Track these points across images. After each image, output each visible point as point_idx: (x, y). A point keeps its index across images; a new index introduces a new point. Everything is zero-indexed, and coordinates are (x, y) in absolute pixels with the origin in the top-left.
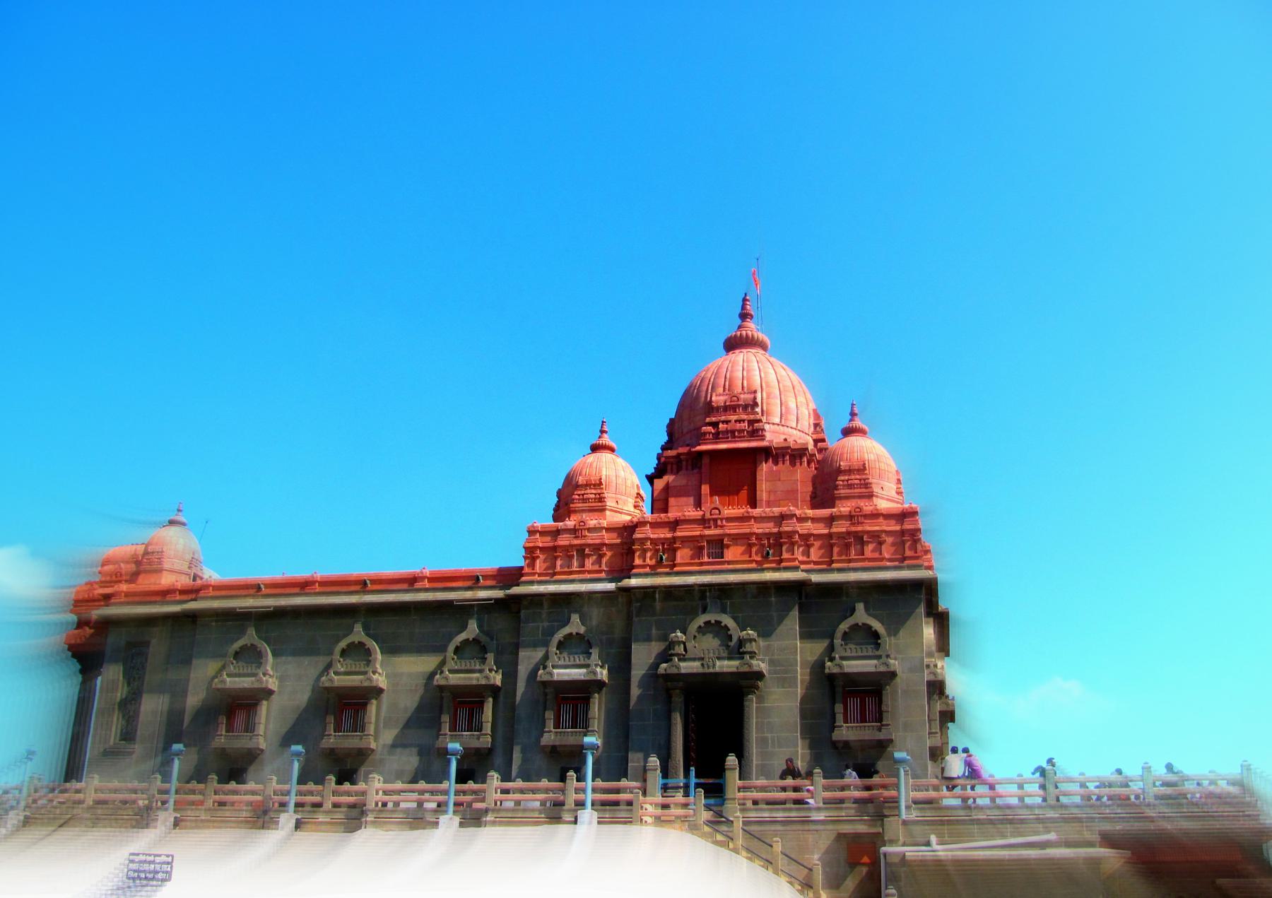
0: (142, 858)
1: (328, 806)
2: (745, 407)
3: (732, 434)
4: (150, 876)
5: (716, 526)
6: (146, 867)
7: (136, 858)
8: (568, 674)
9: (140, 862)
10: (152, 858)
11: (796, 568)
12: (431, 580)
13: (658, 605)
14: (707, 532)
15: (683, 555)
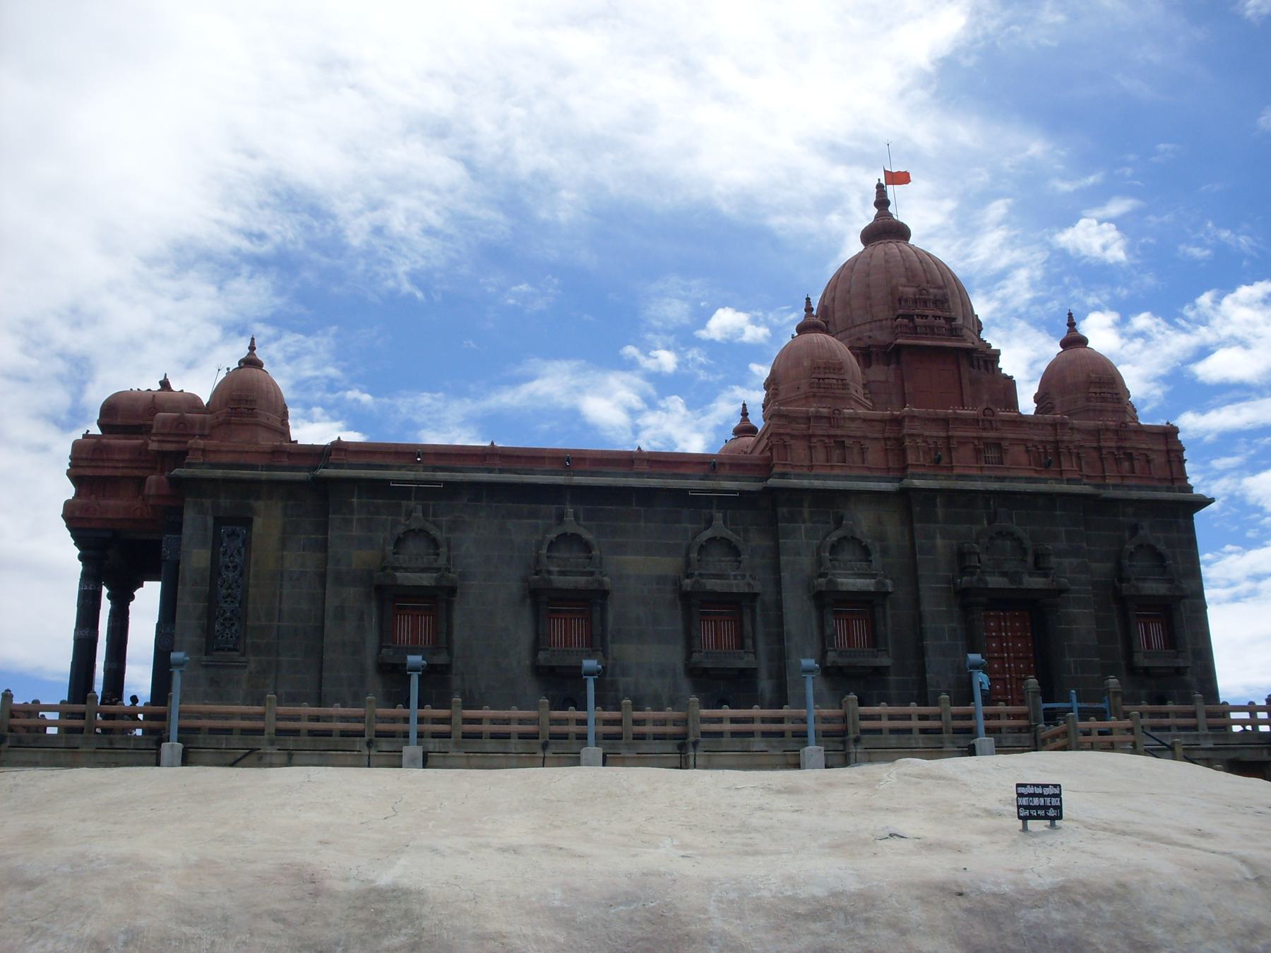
0: (1031, 790)
1: (413, 736)
2: (936, 302)
3: (931, 331)
4: (1041, 813)
5: (992, 429)
6: (1036, 801)
7: (1022, 790)
8: (854, 585)
9: (1030, 795)
10: (1039, 791)
11: (1077, 482)
12: (731, 465)
13: (940, 512)
14: (984, 434)
15: (964, 455)
